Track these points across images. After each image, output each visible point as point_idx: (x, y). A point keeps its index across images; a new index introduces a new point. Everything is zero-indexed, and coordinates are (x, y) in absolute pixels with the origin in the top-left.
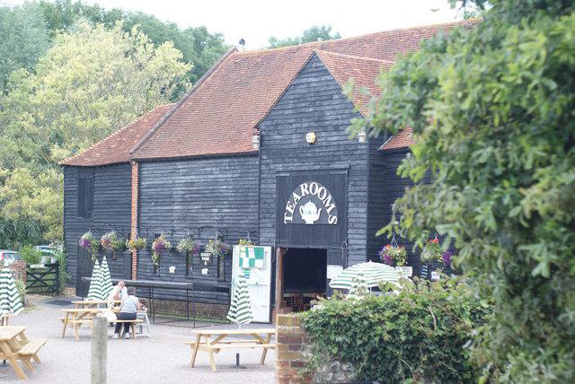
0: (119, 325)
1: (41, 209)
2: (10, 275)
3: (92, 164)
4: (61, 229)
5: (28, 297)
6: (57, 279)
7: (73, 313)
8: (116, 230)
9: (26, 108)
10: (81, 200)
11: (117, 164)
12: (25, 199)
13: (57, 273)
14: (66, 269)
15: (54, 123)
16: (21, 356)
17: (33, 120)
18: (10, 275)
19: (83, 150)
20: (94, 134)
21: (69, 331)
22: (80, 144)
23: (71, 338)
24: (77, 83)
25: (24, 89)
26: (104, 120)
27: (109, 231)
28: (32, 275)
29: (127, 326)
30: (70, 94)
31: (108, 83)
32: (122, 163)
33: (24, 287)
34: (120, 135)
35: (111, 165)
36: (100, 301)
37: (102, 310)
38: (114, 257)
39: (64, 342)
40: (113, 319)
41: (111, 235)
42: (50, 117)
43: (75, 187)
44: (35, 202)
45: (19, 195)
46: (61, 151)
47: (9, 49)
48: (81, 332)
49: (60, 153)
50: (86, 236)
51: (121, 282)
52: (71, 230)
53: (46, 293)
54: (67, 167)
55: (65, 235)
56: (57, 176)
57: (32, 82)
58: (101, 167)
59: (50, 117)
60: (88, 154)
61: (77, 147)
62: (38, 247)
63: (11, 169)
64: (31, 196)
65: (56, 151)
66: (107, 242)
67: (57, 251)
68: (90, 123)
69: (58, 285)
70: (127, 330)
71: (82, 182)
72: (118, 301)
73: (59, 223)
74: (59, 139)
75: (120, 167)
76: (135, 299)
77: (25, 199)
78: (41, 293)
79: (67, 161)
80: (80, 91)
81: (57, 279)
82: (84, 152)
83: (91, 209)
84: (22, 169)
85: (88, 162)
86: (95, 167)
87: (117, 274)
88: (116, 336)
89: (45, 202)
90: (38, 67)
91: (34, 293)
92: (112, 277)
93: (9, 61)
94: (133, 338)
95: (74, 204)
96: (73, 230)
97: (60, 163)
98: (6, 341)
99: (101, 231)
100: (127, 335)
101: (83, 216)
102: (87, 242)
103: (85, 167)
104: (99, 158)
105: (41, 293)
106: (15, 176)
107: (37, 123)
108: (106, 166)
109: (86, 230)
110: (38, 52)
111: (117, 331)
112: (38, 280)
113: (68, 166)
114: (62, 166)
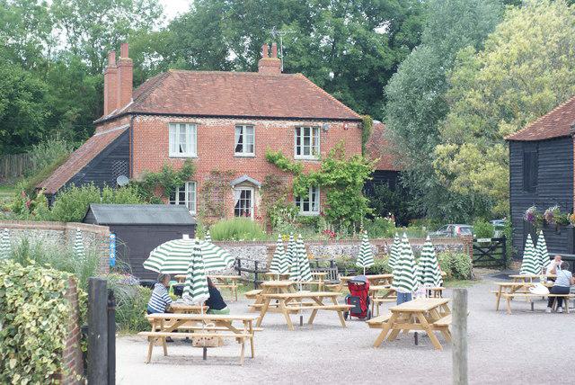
0: (551, 301)
1: (490, 184)
2: (432, 249)
3: (534, 139)
4: (507, 203)
5: (475, 270)
6: (504, 253)
7: (506, 287)
8: (559, 204)
9: (474, 86)
10: (526, 174)
11: (559, 138)
12: (472, 173)
13: (504, 247)
14: (513, 243)
15: (501, 99)
16: (437, 327)
17: (480, 96)
18: (432, 249)
19: (528, 125)
20: (541, 108)
21: (503, 304)
22: (527, 119)
23: (504, 311)
24: (522, 58)
25: (471, 66)
26: (548, 94)
27: (553, 205)
28: (478, 249)
29: (560, 300)
30: (515, 69)
31: (553, 56)
32: (565, 137)
33: (471, 261)
34: (564, 109)
35: (554, 139)
36: (534, 275)
37: (535, 284)
38: (559, 231)
39: (496, 316)
40: (545, 292)
41: (554, 209)
42: (496, 95)
43: (520, 161)
44: (481, 176)
45: (468, 169)
46: (507, 126)
47: (465, 27)
48: (513, 305)
49: (508, 129)
50: (530, 210)
51: (558, 256)
52: (518, 204)
53: (494, 267)
54: (511, 142)
55: (511, 210)
56: (501, 150)
57: (478, 60)
58: (544, 141)
59: (496, 95)
60: (533, 129)
61: (523, 123)
62: (494, 222)
63: (460, 145)
64: (477, 171)
65: (503, 126)
66: (551, 216)
67: (498, 228)
68: (537, 96)
69: (505, 259)
70: (560, 305)
71: (526, 157)
72: (554, 276)
73: (506, 198)
74: (508, 115)
75: (563, 140)
76: (568, 273)
77: (472, 173)
78: (489, 267)
79: (512, 135)
80: (525, 66)
81: (504, 253)
82: (529, 127)
83: (536, 183)
84: (469, 145)
85: (532, 136)
86: (538, 142)
87: (562, 249)
88: (549, 310)
89: (490, 175)
90: (486, 43)
91: (483, 267)
92: (549, 251)
93: (464, 38)
94: (566, 313)
95: (520, 178)
96: (519, 205)
97: (505, 138)
98: (423, 312)
99: (546, 206)
100: (560, 310)
101: (528, 190)
102: (531, 216)
103: (529, 141)
104: (544, 132)
105: (489, 267)
106: (464, 150)
107: (486, 98)
108: (549, 140)
109: (530, 205)
110: (491, 28)
111: (550, 305)
112: (485, 254)
113: (513, 141)
114: (507, 140)
